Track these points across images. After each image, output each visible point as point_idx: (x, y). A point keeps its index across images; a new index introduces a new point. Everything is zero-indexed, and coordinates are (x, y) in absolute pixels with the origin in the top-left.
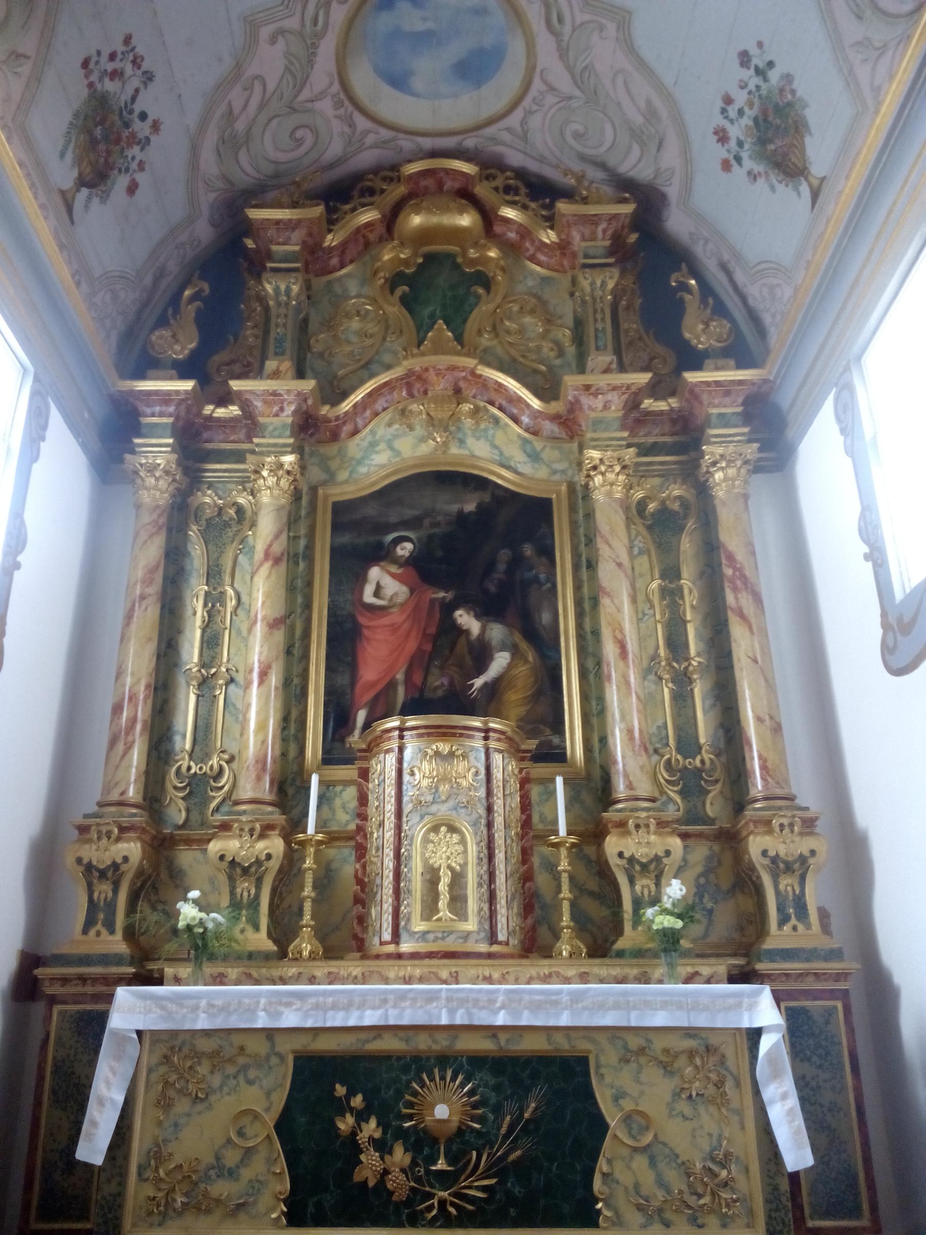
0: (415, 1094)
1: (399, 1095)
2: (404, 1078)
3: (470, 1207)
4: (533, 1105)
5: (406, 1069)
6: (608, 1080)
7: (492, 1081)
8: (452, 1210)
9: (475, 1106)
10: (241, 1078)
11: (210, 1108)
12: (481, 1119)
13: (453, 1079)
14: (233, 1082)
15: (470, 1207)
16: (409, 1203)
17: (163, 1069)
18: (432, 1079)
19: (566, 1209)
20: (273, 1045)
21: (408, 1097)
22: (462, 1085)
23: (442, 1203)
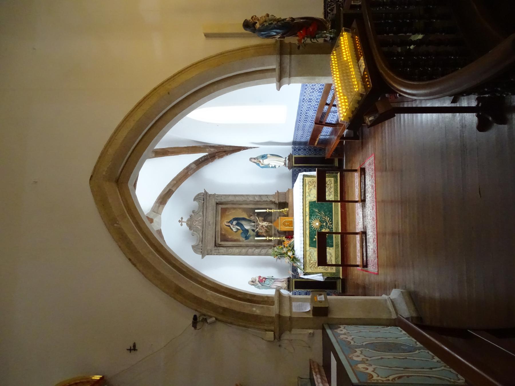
0: (315, 228)
1: (315, 231)
4: (316, 210)
5: (311, 229)
6: (312, 199)
7: (313, 216)
8: (331, 223)
9: (316, 219)
10: (313, 255)
12: (318, 218)
13: (313, 222)
14: (313, 257)
16: (330, 229)
17: (312, 268)
18: (313, 225)
19: (330, 206)
20: (308, 251)
21: (315, 229)
22: (314, 221)
23: (330, 224)
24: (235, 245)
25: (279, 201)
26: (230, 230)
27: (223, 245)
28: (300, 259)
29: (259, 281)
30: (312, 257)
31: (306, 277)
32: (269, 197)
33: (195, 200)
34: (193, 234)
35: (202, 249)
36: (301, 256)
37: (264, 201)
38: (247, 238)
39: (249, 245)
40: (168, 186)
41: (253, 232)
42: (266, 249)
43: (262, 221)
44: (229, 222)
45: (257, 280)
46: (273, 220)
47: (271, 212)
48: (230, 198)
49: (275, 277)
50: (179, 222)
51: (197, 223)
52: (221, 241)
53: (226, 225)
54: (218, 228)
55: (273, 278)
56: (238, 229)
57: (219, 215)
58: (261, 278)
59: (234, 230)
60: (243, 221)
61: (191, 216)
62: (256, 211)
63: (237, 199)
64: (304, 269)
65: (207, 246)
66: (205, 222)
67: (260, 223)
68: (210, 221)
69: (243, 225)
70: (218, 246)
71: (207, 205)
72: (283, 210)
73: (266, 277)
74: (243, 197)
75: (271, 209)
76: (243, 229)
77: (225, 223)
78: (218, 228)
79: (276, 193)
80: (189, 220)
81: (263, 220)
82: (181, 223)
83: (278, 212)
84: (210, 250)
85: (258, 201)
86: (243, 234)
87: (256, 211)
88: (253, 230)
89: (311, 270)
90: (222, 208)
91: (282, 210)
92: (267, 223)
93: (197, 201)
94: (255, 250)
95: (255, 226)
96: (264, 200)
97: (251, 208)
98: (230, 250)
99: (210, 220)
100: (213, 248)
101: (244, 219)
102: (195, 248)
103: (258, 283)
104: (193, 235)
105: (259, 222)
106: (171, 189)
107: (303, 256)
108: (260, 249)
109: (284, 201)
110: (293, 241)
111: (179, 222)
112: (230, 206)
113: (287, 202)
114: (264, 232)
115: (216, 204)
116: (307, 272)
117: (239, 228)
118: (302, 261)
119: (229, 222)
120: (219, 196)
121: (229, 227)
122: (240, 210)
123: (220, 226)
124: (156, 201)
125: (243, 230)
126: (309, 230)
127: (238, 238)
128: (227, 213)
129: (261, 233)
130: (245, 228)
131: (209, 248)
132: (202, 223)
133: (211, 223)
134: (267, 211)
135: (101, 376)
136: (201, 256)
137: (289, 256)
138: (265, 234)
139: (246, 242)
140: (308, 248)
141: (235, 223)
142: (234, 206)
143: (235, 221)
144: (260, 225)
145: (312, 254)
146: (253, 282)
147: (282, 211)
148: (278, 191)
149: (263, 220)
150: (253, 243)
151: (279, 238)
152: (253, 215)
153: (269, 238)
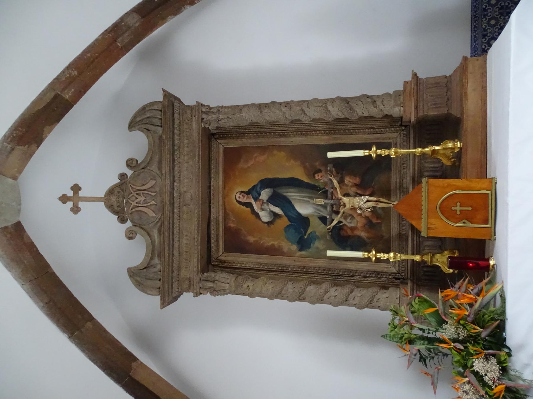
24: (266, 264)
25: (421, 114)
26: (253, 217)
32: (379, 103)
33: (132, 125)
34: (131, 235)
37: (362, 119)
39: (309, 268)
40: (51, 86)
42: (367, 286)
43: (354, 189)
44: (248, 193)
46: (393, 187)
47: (389, 155)
48: (244, 114)
51: (141, 199)
52: (227, 249)
56: (275, 215)
57: (217, 173)
59: (265, 217)
61: (123, 176)
62: (331, 155)
63: (269, 116)
65: (179, 269)
67: (345, 200)
68: (185, 192)
69: (293, 202)
70: (217, 266)
71: (176, 142)
72: (437, 148)
74: (284, 109)
75: (388, 147)
77: (238, 195)
78: (217, 212)
79: (406, 83)
81: (356, 185)
84: (190, 279)
85: (338, 121)
86: (292, 231)
87: (331, 155)
88: (323, 219)
90: (225, 149)
91: (432, 148)
92: (371, 198)
93: (139, 129)
94: (326, 291)
95: (329, 209)
96: (360, 114)
97: (318, 146)
98: (249, 283)
99: (185, 189)
101: (294, 183)
102: (138, 279)
104: (130, 238)
106: (59, 95)
108: (346, 290)
109: (443, 111)
112: (250, 141)
113: (455, 112)
114: (360, 225)
115: (209, 139)
117: (277, 210)
119: (248, 193)
120: (209, 110)
121: (249, 209)
122: (282, 154)
123: (221, 208)
124: (5, 136)
125: (290, 219)
127: (276, 243)
128: (242, 165)
129: (353, 229)
130: (299, 214)
134: (370, 155)
136: (157, 299)
137: (476, 374)
138: (363, 234)
139: (301, 256)
141: (265, 194)
142: (263, 141)
143: (265, 190)
144: (345, 205)
147: (434, 151)
148: (415, 75)
149: (356, 185)
151: (417, 258)
152: (322, 168)
153: (379, 255)
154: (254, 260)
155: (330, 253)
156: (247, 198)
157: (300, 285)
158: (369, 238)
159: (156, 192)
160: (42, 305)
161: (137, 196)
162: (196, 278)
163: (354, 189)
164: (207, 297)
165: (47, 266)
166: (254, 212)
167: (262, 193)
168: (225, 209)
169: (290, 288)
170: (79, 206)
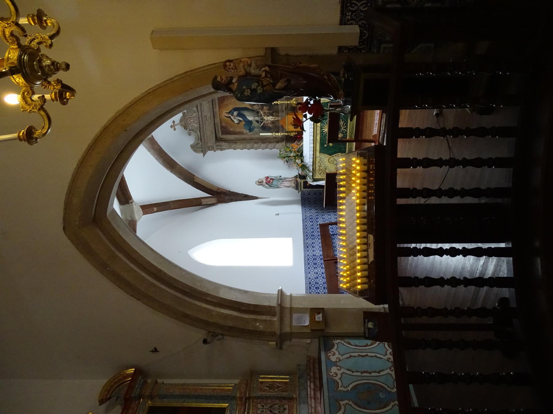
2: (324, 135)
3: (345, 124)
11: (328, 166)
13: (324, 126)
14: (324, 163)
15: (345, 124)
16: (343, 134)
17: (321, 174)
18: (324, 130)
23: (344, 128)
24: (238, 138)
27: (224, 138)
28: (309, 167)
29: (266, 183)
30: (322, 164)
31: (315, 183)
35: (202, 148)
36: (310, 164)
38: (251, 130)
39: (254, 138)
41: (257, 123)
44: (229, 113)
45: (265, 181)
49: (283, 177)
50: (172, 128)
51: (192, 121)
53: (226, 117)
54: (218, 121)
55: (281, 178)
56: (240, 121)
57: (216, 105)
58: (269, 180)
59: (236, 121)
60: (246, 111)
64: (313, 176)
65: (207, 143)
66: (202, 117)
67: (265, 118)
68: (206, 115)
73: (274, 178)
76: (246, 120)
77: (225, 114)
78: (218, 121)
80: (182, 120)
81: (267, 109)
82: (173, 128)
83: (285, 104)
89: (320, 176)
92: (273, 117)
94: (260, 145)
99: (206, 114)
100: (214, 145)
103: (265, 184)
104: (190, 135)
105: (263, 116)
107: (312, 163)
110: (302, 146)
111: (172, 128)
114: (269, 123)
116: (316, 179)
118: (311, 169)
119: (229, 113)
121: (230, 119)
125: (245, 122)
126: (320, 136)
127: (241, 131)
128: (225, 103)
129: (267, 124)
130: (249, 120)
131: (209, 144)
132: (198, 120)
133: (208, 117)
135: (134, 369)
138: (271, 126)
140: (318, 154)
141: (235, 113)
143: (236, 112)
145: (322, 160)
146: (260, 182)
149: (267, 109)
150: (257, 136)
153: (276, 134)
154: (234, 137)
155: (261, 134)
156: (229, 115)
157: (252, 144)
158: (272, 127)
159: (196, 117)
160: (161, 161)
161: (190, 120)
162: (215, 146)
163: (267, 111)
164: (219, 152)
165: (161, 148)
166: (232, 120)
167: (234, 113)
168: (220, 119)
169: (248, 145)
170: (176, 128)
